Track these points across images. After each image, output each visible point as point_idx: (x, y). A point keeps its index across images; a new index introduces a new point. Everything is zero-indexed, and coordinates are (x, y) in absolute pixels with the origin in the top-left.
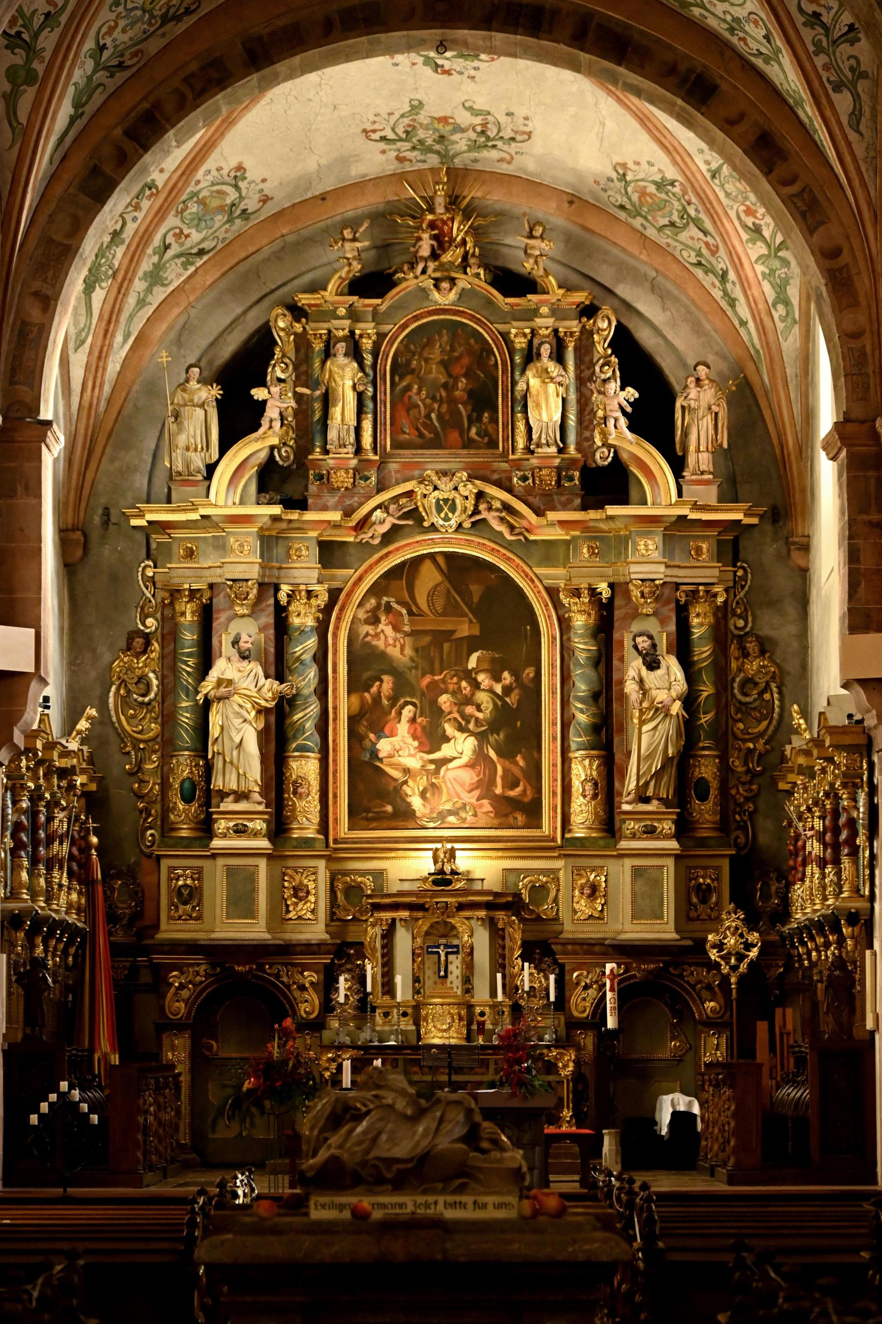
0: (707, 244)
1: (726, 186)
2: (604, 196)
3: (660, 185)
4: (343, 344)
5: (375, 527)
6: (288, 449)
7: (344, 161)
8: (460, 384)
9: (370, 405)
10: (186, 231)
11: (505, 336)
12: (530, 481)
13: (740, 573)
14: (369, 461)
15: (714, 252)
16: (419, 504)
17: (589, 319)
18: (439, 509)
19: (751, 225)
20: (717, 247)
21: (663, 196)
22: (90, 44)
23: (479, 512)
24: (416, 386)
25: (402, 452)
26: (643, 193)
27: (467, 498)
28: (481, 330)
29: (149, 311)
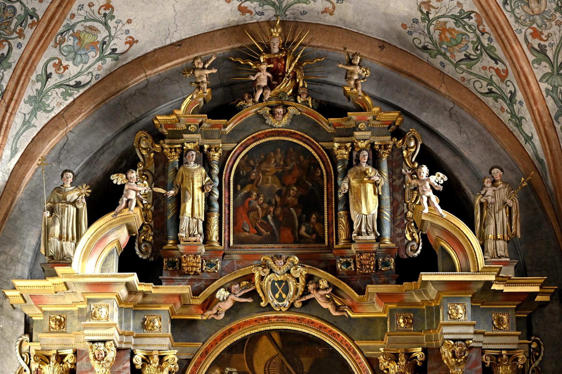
0: (497, 71)
1: (517, 11)
2: (410, 38)
3: (457, 19)
4: (194, 153)
5: (219, 304)
6: (147, 244)
8: (292, 192)
9: (217, 206)
10: (65, 63)
11: (330, 152)
12: (352, 266)
13: (534, 345)
14: (216, 250)
15: (503, 77)
16: (258, 286)
17: (398, 140)
18: (275, 290)
19: (536, 47)
20: (507, 72)
21: (461, 29)
23: (310, 293)
24: (255, 194)
25: (243, 246)
26: (443, 29)
27: (297, 280)
28: (309, 148)
29: (33, 133)
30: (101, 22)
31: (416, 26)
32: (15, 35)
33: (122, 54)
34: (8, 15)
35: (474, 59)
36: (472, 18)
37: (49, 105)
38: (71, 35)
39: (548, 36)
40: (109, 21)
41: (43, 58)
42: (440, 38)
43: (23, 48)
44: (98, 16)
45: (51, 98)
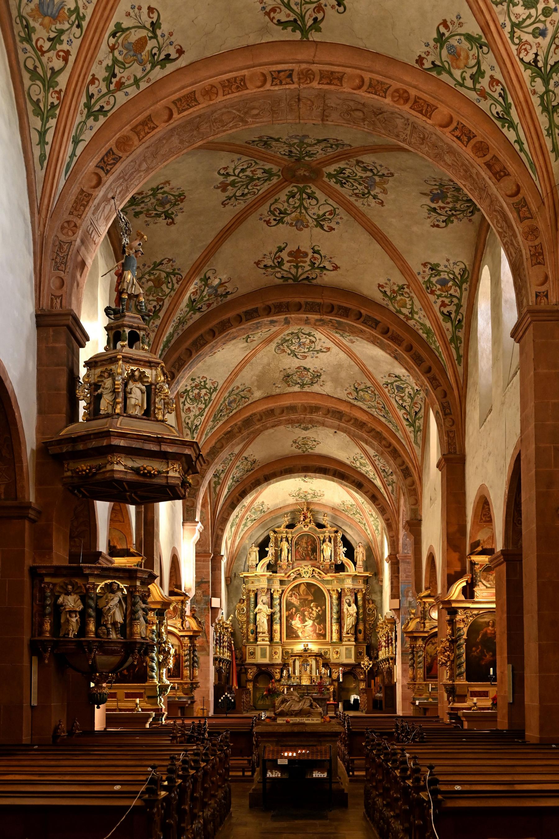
7: (285, 500)
22: (231, 476)
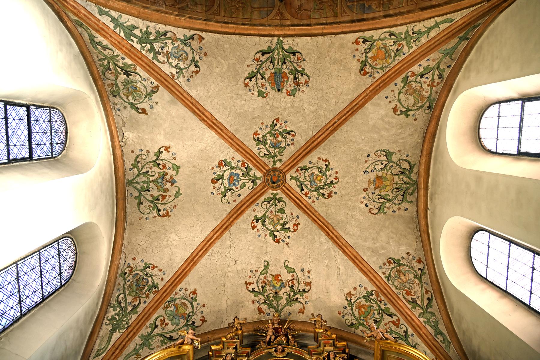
0: (393, 322)
1: (395, 283)
3: (366, 298)
10: (167, 321)
15: (397, 324)
19: (411, 300)
20: (398, 320)
21: (369, 304)
26: (360, 307)
30: (189, 302)
31: (346, 310)
32: (144, 296)
33: (198, 327)
34: (144, 283)
35: (379, 321)
36: (373, 295)
37: (152, 345)
38: (173, 305)
39: (415, 293)
40: (194, 303)
41: (155, 314)
42: (359, 314)
43: (146, 305)
44: (189, 298)
45: (154, 341)
